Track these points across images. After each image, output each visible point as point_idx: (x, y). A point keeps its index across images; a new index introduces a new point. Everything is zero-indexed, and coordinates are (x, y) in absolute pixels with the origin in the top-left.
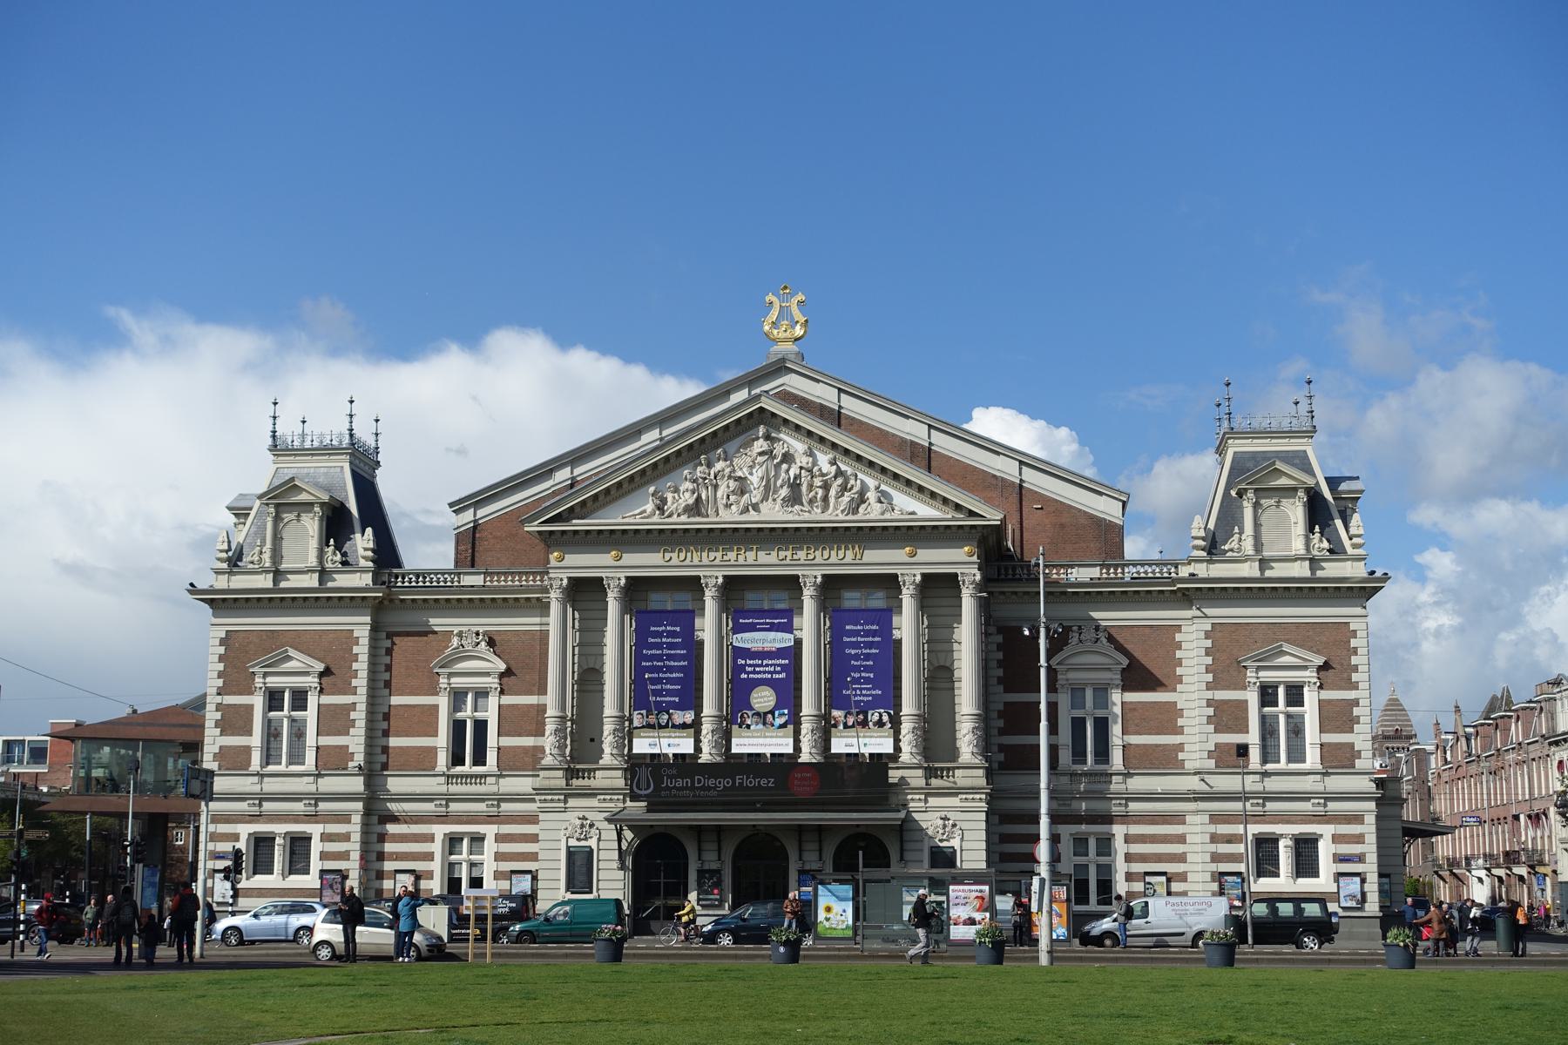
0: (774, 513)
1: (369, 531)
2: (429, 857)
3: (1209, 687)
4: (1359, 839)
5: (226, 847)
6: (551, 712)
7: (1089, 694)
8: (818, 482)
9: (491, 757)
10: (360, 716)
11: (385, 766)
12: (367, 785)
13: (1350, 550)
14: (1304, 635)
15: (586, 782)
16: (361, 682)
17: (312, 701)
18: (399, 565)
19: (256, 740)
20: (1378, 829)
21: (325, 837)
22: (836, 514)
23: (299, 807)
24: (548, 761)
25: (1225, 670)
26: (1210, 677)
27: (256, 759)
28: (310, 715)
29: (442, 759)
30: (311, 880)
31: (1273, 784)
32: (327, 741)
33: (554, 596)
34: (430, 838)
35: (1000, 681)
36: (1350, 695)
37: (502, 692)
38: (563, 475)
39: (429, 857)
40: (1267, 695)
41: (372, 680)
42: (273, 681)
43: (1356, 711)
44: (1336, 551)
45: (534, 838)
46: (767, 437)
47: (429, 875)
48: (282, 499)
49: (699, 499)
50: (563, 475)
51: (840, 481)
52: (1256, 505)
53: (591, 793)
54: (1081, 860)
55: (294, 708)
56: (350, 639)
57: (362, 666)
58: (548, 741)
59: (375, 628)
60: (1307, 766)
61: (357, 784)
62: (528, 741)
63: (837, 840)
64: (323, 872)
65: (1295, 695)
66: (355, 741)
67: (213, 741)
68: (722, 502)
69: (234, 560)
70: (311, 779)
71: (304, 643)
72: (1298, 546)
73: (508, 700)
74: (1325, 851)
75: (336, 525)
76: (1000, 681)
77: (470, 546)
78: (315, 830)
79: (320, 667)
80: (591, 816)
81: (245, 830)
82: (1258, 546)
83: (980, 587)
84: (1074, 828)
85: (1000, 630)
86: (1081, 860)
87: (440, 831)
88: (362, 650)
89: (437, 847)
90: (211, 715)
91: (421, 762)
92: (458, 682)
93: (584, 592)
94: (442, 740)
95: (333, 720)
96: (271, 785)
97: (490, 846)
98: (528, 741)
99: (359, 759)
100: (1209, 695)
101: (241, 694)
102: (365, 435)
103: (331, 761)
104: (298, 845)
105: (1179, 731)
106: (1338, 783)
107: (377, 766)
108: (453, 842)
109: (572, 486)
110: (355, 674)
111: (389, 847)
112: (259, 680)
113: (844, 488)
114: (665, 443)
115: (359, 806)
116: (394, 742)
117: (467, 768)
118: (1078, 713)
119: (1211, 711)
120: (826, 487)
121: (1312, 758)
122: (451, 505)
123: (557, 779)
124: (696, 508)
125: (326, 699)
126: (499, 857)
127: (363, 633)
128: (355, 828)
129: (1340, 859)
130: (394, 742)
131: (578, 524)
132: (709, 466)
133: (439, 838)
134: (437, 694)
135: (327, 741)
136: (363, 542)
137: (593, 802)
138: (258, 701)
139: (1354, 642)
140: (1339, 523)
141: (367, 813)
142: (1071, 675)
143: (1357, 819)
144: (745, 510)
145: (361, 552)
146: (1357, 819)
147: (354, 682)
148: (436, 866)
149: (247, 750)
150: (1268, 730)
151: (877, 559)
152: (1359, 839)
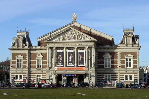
0: (72, 40)
1: (28, 42)
2: (35, 77)
3: (120, 59)
4: (137, 76)
5: (13, 76)
6: (47, 62)
7: (107, 59)
8: (77, 36)
9: (42, 67)
10: (27, 62)
11: (31, 68)
12: (28, 70)
13: (137, 43)
14: (131, 53)
15: (51, 69)
16: (27, 58)
17: (22, 60)
18: (32, 45)
20: (139, 74)
21: (24, 75)
22: (79, 40)
23: (21, 72)
24: (47, 67)
25: (122, 57)
26: (121, 58)
27: (16, 67)
28: (22, 62)
29: (36, 67)
30: (22, 80)
32: (23, 65)
33: (48, 49)
34: (35, 75)
35: (97, 58)
36: (137, 60)
37: (43, 59)
38: (49, 35)
39: (35, 77)
40: (127, 60)
41: (29, 58)
42: (18, 58)
43: (137, 62)
44: (135, 43)
45: (46, 75)
46: (71, 32)
48: (18, 38)
49: (63, 38)
50: (49, 35)
51: (79, 36)
52: (127, 38)
53: (52, 70)
54: (106, 78)
55: (20, 61)
56: (26, 54)
57: (27, 57)
58: (47, 65)
59: (29, 52)
60: (131, 68)
61: (27, 69)
62: (45, 65)
63: (78, 76)
64: (24, 79)
65: (130, 60)
66: (27, 65)
67: (11, 65)
68: (66, 39)
69: (13, 45)
71: (21, 54)
72: (131, 43)
73: (43, 60)
74: (133, 77)
75: (24, 41)
76: (97, 58)
77: (39, 44)
78: (23, 75)
80: (53, 73)
81: (15, 75)
82: (127, 43)
83: (94, 48)
84: (106, 74)
85: (98, 53)
86: (106, 78)
87: (36, 75)
88: (27, 55)
89: (36, 76)
90: (11, 62)
91: (34, 67)
92: (38, 58)
93: (51, 48)
94: (36, 65)
95: (24, 63)
96: (18, 70)
97: (42, 76)
98: (45, 65)
99: (27, 67)
100: (121, 60)
102: (27, 31)
103: (24, 67)
104: (21, 76)
105: (117, 64)
106: (135, 69)
107: (30, 67)
108: (38, 76)
109: (50, 36)
111: (31, 76)
112: (16, 58)
113: (79, 37)
114: (61, 31)
115: (27, 72)
116: (32, 65)
117: (39, 68)
118: (106, 62)
119: (121, 62)
120: (78, 37)
122: (37, 38)
123: (48, 69)
124: (63, 39)
125: (23, 60)
126: (43, 77)
127: (27, 53)
128: (27, 74)
129: (134, 78)
130: (32, 65)
131: (50, 41)
132: (65, 35)
133: (36, 75)
134: (35, 59)
135: (23, 65)
136: (27, 43)
137: (52, 71)
139: (137, 54)
140: (136, 40)
141: (28, 73)
142: (105, 58)
143: (137, 74)
144: (69, 40)
145: (27, 44)
146: (137, 74)
148: (36, 78)
149: (15, 66)
150: (127, 63)
151: (83, 45)
152: (137, 76)
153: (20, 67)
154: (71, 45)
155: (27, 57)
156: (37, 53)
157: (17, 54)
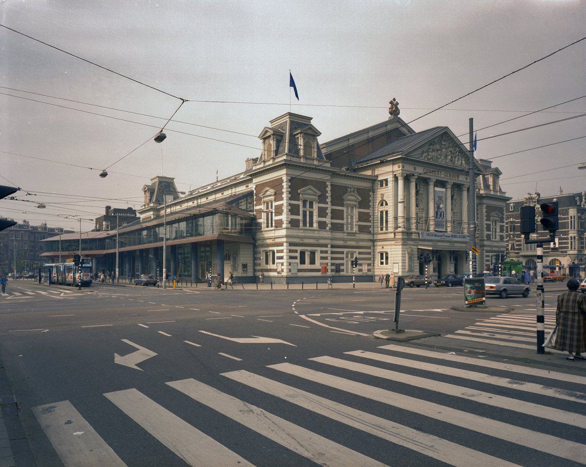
2: (342, 259)
10: (329, 211)
16: (329, 200)
19: (300, 217)
27: (301, 224)
31: (495, 244)
34: (342, 253)
39: (342, 259)
47: (343, 265)
70: (317, 232)
79: (319, 193)
81: (299, 249)
87: (345, 250)
89: (344, 256)
101: (295, 200)
110: (327, 197)
121: (498, 238)
127: (328, 184)
134: (342, 205)
138: (300, 203)
147: (327, 200)
153: (311, 225)
154: (442, 176)
155: (327, 195)
156: (348, 187)
157: (305, 182)
